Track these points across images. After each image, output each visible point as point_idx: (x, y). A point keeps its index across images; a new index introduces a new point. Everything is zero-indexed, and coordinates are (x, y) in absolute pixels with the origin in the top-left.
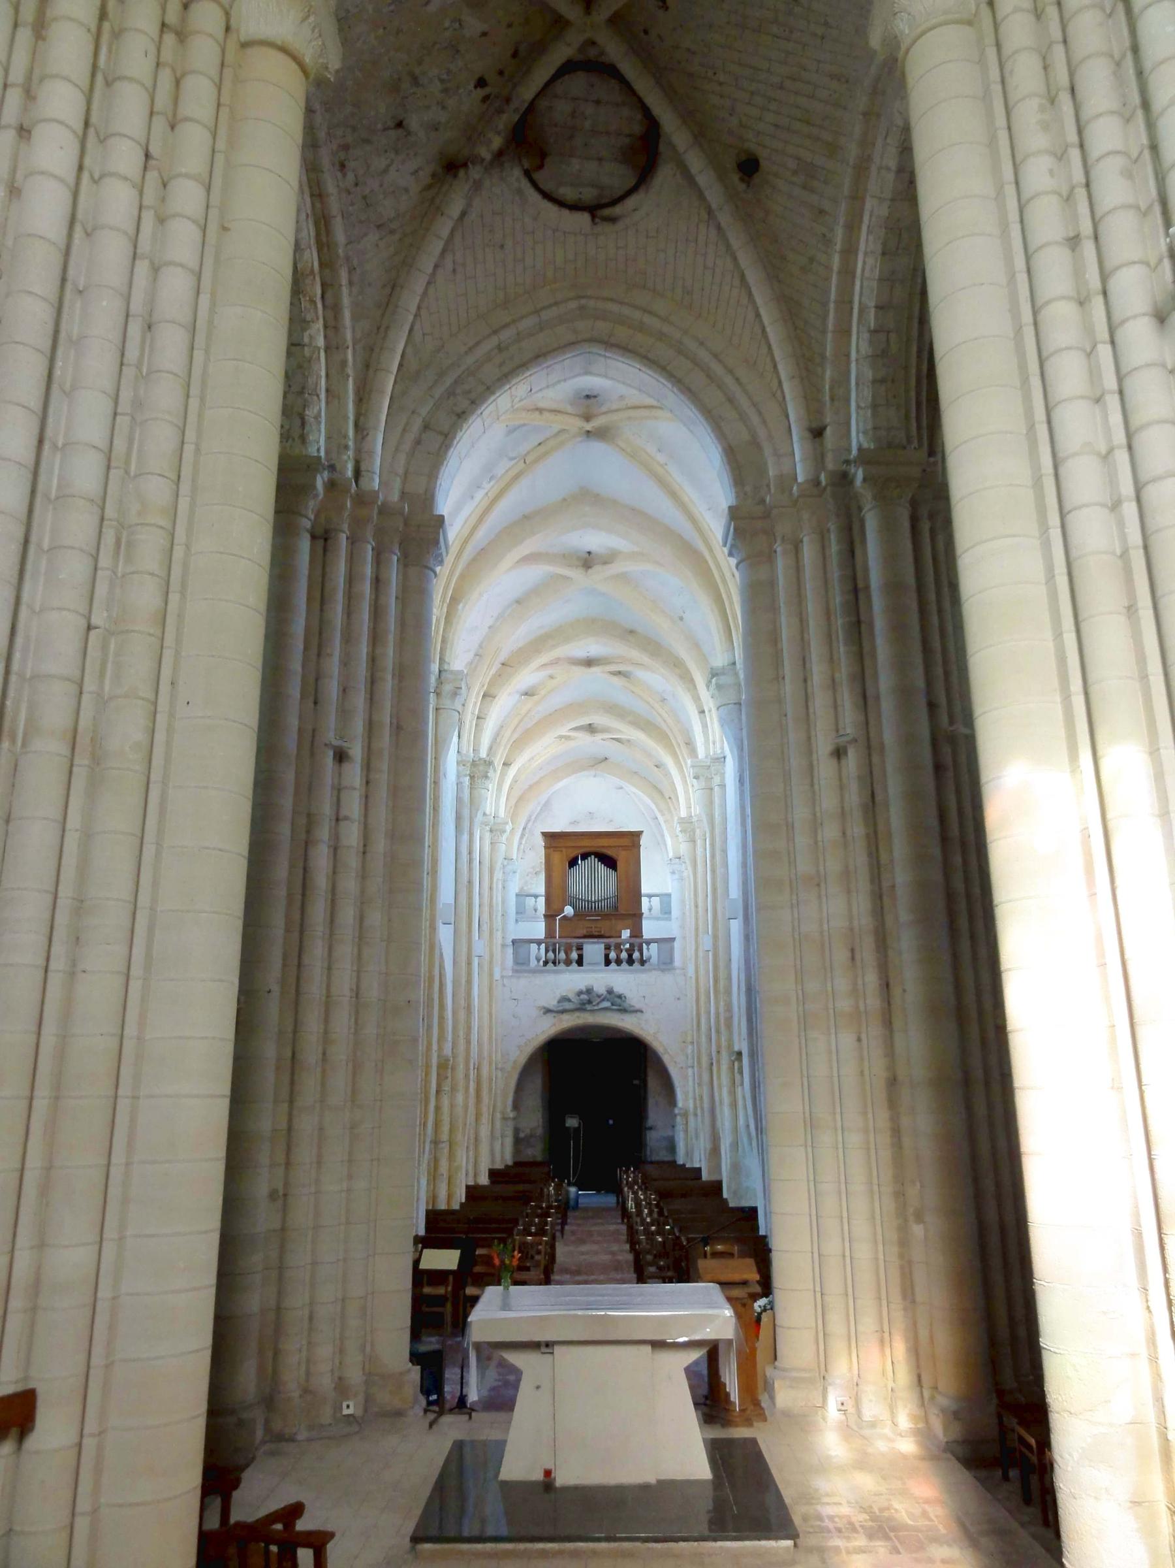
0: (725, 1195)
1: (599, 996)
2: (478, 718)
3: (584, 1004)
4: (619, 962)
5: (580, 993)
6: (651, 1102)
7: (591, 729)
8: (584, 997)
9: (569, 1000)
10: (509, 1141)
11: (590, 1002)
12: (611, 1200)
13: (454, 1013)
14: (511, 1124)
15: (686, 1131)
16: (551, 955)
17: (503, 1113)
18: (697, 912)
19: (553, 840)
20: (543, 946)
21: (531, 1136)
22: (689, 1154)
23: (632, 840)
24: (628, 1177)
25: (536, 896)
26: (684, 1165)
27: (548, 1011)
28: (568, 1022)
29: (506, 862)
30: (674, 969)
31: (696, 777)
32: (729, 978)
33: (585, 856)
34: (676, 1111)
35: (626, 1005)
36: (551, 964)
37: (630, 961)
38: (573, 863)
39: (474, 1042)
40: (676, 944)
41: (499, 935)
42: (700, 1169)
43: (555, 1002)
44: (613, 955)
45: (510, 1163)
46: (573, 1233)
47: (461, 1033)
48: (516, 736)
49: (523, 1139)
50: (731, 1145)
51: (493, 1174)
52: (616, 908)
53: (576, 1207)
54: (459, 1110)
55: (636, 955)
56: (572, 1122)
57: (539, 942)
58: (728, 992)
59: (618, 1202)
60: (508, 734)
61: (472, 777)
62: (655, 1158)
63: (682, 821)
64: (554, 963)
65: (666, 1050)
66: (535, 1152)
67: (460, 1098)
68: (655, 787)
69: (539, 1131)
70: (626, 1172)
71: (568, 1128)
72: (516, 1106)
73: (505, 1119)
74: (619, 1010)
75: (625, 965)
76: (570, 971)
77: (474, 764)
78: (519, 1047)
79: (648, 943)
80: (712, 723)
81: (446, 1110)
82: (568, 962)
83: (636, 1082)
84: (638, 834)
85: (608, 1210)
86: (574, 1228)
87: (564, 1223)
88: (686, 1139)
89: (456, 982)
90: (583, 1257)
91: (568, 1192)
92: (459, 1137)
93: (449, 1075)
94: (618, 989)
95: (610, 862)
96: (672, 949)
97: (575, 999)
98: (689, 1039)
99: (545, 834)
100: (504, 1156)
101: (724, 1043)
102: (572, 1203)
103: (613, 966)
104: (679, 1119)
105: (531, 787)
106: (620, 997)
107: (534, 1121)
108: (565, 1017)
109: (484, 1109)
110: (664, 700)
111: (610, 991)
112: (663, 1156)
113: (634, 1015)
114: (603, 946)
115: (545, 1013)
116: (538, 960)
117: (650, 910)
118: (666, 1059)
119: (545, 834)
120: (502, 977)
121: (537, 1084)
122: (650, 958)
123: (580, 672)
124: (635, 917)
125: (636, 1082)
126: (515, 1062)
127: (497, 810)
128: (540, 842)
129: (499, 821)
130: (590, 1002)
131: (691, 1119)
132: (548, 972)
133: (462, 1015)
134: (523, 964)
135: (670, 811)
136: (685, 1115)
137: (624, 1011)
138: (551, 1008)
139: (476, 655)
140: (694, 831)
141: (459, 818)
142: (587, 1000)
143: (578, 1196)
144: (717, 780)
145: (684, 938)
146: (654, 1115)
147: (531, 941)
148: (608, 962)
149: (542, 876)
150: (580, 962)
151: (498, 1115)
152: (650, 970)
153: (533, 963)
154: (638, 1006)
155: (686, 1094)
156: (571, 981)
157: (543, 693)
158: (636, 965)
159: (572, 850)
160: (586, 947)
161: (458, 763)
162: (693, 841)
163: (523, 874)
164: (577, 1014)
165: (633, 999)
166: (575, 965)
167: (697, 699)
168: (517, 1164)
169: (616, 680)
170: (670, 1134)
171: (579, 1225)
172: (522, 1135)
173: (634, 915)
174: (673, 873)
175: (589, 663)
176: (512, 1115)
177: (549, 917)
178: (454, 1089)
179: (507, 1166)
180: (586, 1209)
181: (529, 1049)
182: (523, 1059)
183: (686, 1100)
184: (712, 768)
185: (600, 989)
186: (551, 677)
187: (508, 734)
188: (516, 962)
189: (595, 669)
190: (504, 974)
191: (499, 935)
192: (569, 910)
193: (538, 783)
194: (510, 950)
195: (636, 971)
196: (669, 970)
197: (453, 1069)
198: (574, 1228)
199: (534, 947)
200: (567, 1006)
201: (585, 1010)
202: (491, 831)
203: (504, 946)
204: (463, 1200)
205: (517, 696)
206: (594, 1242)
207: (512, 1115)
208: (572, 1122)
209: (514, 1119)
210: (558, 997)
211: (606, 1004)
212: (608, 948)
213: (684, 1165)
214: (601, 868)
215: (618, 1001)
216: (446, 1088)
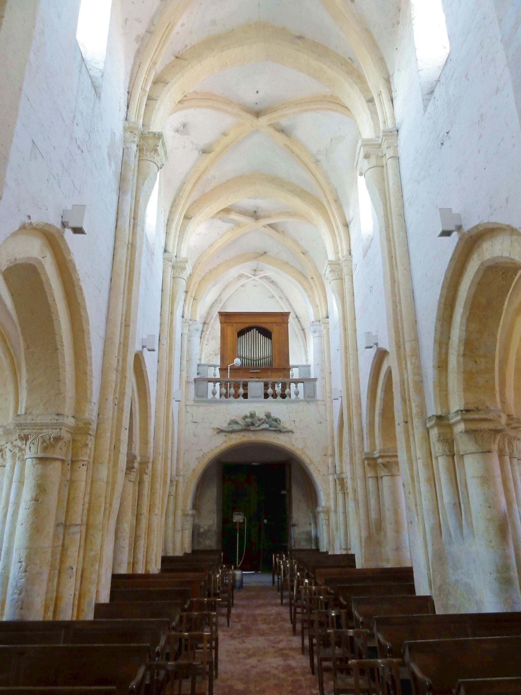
0: (422, 588)
1: (260, 420)
2: (149, 98)
3: (249, 426)
4: (275, 396)
5: (246, 417)
6: (294, 505)
7: (255, 215)
8: (249, 420)
9: (237, 423)
10: (188, 533)
11: (253, 424)
12: (265, 579)
13: (104, 372)
14: (190, 519)
15: (328, 525)
16: (224, 390)
17: (183, 511)
18: (345, 335)
19: (226, 317)
20: (218, 384)
21: (209, 531)
22: (331, 543)
23: (282, 318)
24: (285, 564)
25: (215, 366)
26: (327, 552)
27: (220, 431)
28: (236, 439)
29: (191, 322)
30: (317, 401)
31: (367, 156)
32: (416, 340)
33: (249, 329)
34: (320, 509)
35: (280, 427)
36: (223, 397)
37: (283, 396)
38: (241, 333)
39: (151, 440)
40: (318, 383)
41: (184, 373)
42: (354, 555)
43: (226, 425)
44: (270, 391)
45: (189, 551)
46: (239, 616)
47: (111, 397)
48: (195, 195)
49: (203, 533)
50: (432, 529)
51: (165, 560)
52: (271, 364)
53: (241, 587)
54: (101, 487)
55: (287, 391)
56: (238, 518)
57: (215, 381)
58: (416, 353)
59: (274, 582)
60: (188, 187)
61: (140, 149)
62: (297, 547)
63: (331, 263)
64: (226, 396)
65: (311, 461)
66: (211, 543)
67: (104, 473)
68: (301, 273)
69: (215, 528)
70: (281, 558)
71: (236, 523)
72: (196, 506)
73: (185, 515)
74: (275, 431)
75: (279, 398)
76: (238, 402)
77: (143, 137)
78: (197, 459)
79: (296, 382)
80: (382, 105)
81: (82, 485)
82: (236, 396)
83: (283, 492)
84: (287, 314)
85: (264, 589)
86: (239, 611)
87: (230, 606)
88: (328, 531)
89: (108, 340)
90: (253, 661)
91: (234, 575)
92: (99, 518)
93: (91, 445)
94: (274, 415)
95: (266, 333)
96: (314, 386)
97: (241, 422)
98: (330, 452)
99: (221, 314)
100: (181, 545)
101: (415, 410)
102: (238, 584)
103: (270, 398)
104: (322, 517)
105: (211, 271)
106: (276, 420)
107: (210, 521)
108: (233, 436)
109: (158, 501)
110: (317, 161)
111: (268, 416)
112: (304, 545)
113: (286, 434)
114: (263, 384)
115: (218, 433)
116: (214, 394)
117: (292, 376)
118: (312, 469)
119: (221, 314)
120: (186, 405)
121: (212, 494)
122: (297, 394)
123: (249, 120)
124: (286, 369)
125: (283, 492)
126: (194, 470)
127: (179, 250)
128: (216, 326)
129: (178, 259)
130: (253, 424)
131: (332, 515)
132: (221, 402)
133: (113, 376)
134: (202, 396)
135: (311, 288)
136: (327, 512)
137: (280, 431)
138: (223, 428)
139: (148, 32)
140: (341, 270)
141: (122, 179)
142: (250, 423)
143: (242, 575)
144: (389, 153)
145: (323, 378)
146: (298, 514)
147: (210, 381)
148: (266, 396)
149: (219, 356)
150: (245, 396)
151: (179, 513)
152: (297, 401)
153: (210, 396)
154: (289, 428)
155: (328, 495)
156: (239, 409)
157: (218, 149)
158: (287, 398)
159: (241, 326)
160: (249, 384)
161: (125, 129)
162: (341, 279)
163: (207, 351)
164: (243, 434)
165: (286, 423)
166: (241, 398)
167: (364, 88)
168: (194, 552)
169: (280, 138)
170: (307, 528)
171: (243, 607)
172: (202, 530)
173: (285, 369)
174: (315, 332)
175: (258, 114)
176: (190, 512)
177: (223, 370)
178: (96, 460)
179: (186, 554)
180: (250, 589)
181: (206, 461)
182: (200, 470)
183: (328, 500)
184: (384, 146)
185: (261, 414)
186: (225, 134)
187: (188, 187)
188: (197, 395)
189: (263, 120)
190: (188, 403)
191: (184, 373)
192: (237, 361)
193: (214, 269)
194: (192, 387)
195: (288, 402)
196: (313, 401)
197: (97, 437)
198: (239, 611)
199: (211, 385)
200: (236, 427)
201: (249, 430)
202: (173, 267)
203: (188, 382)
204: (105, 598)
205: (196, 154)
206: (263, 634)
207: (190, 512)
208: (238, 518)
209: (193, 516)
210: (228, 421)
211: (265, 426)
212: (266, 385)
213: (327, 552)
214: (261, 337)
215: (274, 423)
216: (86, 456)
